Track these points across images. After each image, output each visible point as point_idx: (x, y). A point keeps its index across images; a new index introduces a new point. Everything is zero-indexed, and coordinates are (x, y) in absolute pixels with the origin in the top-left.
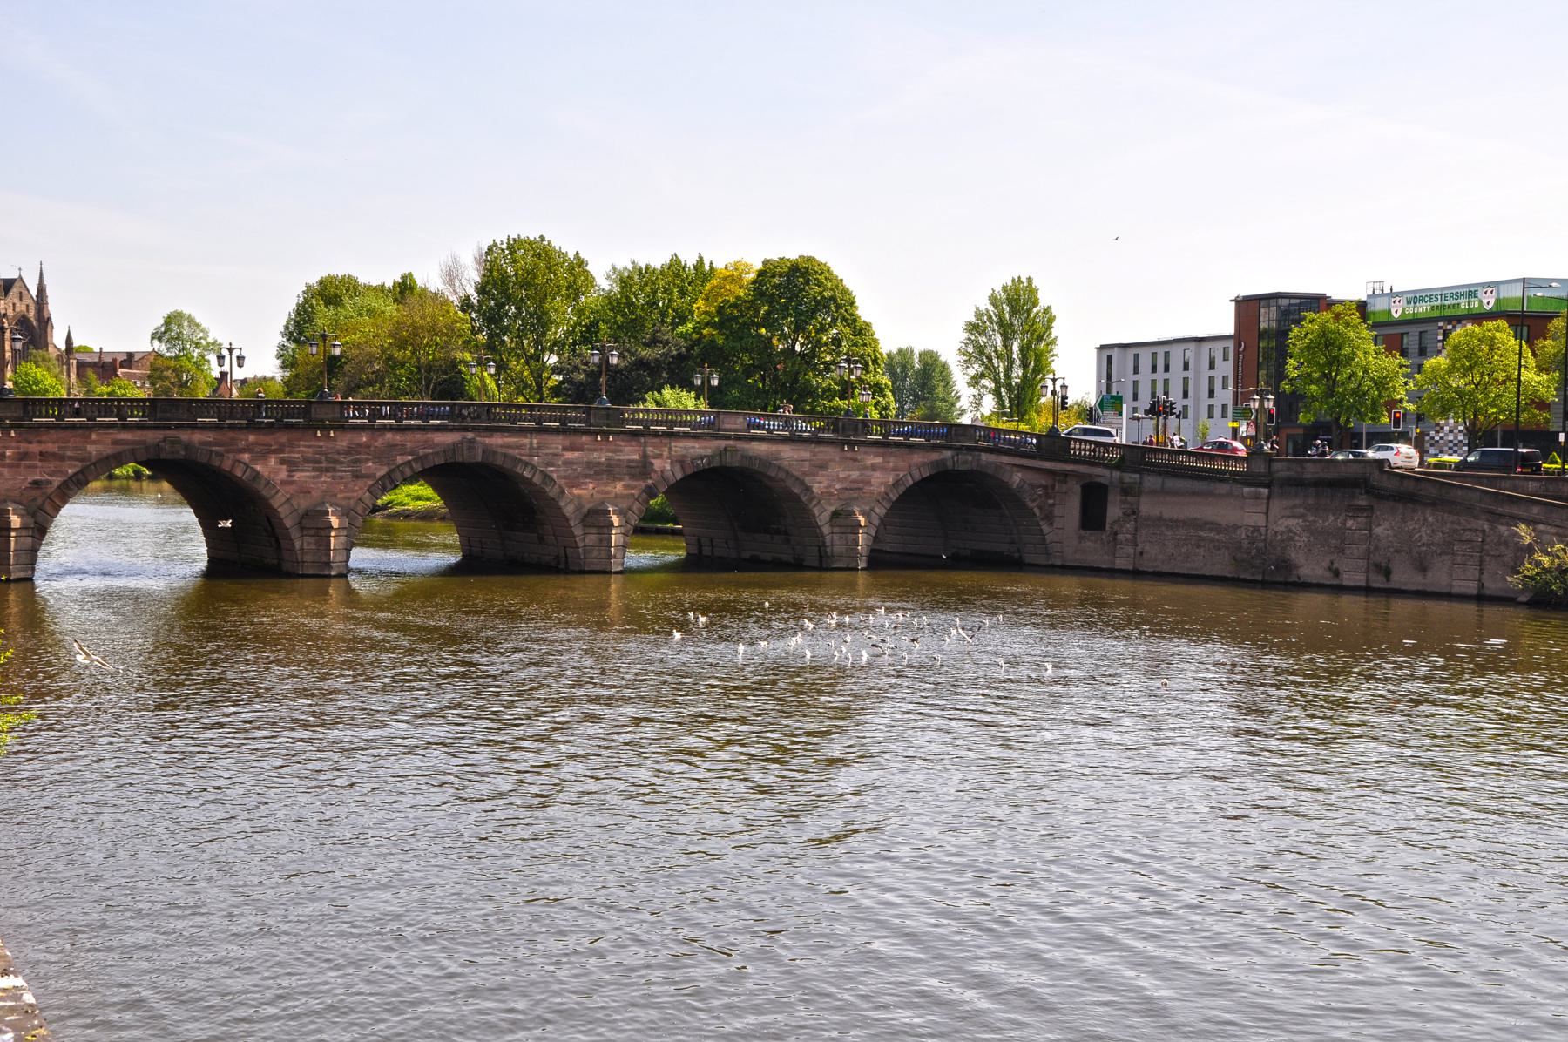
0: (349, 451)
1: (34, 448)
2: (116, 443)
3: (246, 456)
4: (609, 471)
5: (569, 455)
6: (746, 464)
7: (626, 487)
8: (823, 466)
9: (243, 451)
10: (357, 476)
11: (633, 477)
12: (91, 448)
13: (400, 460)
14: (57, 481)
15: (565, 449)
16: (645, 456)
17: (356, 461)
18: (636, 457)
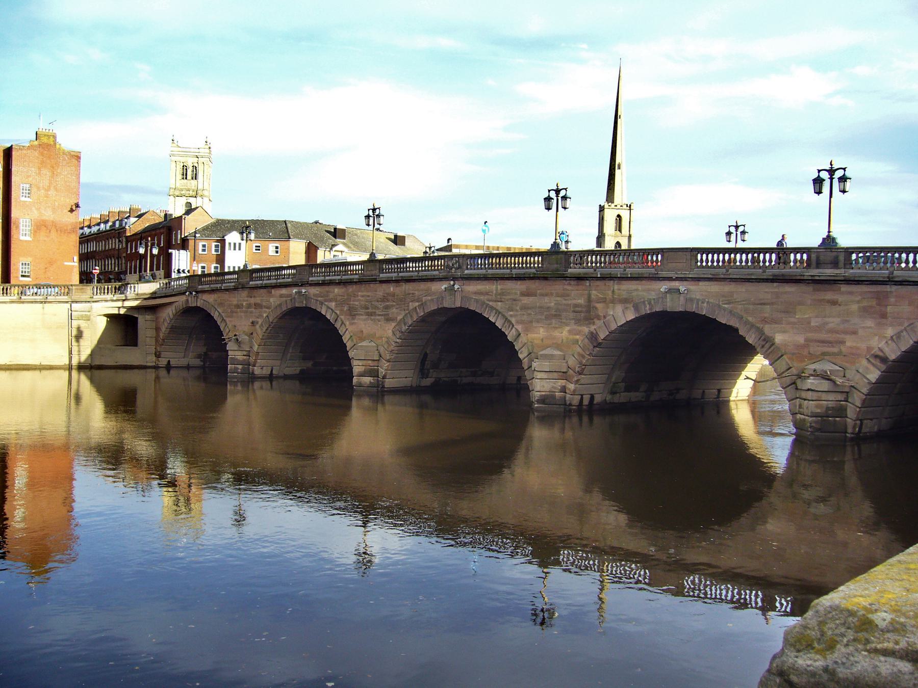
0: (384, 299)
1: (252, 301)
2: (281, 296)
3: (332, 305)
4: (554, 316)
5: (526, 300)
6: (693, 308)
7: (570, 332)
8: (789, 310)
9: (330, 301)
10: (388, 320)
11: (578, 322)
12: (272, 300)
13: (413, 305)
14: (260, 321)
15: (523, 294)
16: (589, 300)
17: (387, 307)
18: (581, 301)
